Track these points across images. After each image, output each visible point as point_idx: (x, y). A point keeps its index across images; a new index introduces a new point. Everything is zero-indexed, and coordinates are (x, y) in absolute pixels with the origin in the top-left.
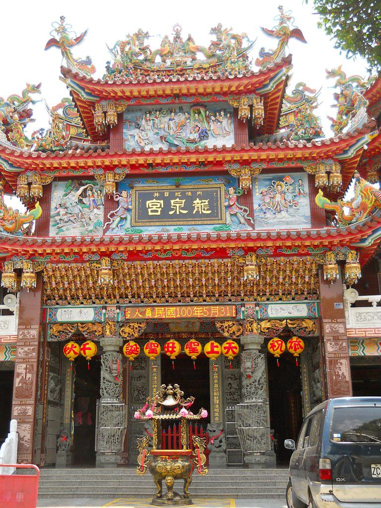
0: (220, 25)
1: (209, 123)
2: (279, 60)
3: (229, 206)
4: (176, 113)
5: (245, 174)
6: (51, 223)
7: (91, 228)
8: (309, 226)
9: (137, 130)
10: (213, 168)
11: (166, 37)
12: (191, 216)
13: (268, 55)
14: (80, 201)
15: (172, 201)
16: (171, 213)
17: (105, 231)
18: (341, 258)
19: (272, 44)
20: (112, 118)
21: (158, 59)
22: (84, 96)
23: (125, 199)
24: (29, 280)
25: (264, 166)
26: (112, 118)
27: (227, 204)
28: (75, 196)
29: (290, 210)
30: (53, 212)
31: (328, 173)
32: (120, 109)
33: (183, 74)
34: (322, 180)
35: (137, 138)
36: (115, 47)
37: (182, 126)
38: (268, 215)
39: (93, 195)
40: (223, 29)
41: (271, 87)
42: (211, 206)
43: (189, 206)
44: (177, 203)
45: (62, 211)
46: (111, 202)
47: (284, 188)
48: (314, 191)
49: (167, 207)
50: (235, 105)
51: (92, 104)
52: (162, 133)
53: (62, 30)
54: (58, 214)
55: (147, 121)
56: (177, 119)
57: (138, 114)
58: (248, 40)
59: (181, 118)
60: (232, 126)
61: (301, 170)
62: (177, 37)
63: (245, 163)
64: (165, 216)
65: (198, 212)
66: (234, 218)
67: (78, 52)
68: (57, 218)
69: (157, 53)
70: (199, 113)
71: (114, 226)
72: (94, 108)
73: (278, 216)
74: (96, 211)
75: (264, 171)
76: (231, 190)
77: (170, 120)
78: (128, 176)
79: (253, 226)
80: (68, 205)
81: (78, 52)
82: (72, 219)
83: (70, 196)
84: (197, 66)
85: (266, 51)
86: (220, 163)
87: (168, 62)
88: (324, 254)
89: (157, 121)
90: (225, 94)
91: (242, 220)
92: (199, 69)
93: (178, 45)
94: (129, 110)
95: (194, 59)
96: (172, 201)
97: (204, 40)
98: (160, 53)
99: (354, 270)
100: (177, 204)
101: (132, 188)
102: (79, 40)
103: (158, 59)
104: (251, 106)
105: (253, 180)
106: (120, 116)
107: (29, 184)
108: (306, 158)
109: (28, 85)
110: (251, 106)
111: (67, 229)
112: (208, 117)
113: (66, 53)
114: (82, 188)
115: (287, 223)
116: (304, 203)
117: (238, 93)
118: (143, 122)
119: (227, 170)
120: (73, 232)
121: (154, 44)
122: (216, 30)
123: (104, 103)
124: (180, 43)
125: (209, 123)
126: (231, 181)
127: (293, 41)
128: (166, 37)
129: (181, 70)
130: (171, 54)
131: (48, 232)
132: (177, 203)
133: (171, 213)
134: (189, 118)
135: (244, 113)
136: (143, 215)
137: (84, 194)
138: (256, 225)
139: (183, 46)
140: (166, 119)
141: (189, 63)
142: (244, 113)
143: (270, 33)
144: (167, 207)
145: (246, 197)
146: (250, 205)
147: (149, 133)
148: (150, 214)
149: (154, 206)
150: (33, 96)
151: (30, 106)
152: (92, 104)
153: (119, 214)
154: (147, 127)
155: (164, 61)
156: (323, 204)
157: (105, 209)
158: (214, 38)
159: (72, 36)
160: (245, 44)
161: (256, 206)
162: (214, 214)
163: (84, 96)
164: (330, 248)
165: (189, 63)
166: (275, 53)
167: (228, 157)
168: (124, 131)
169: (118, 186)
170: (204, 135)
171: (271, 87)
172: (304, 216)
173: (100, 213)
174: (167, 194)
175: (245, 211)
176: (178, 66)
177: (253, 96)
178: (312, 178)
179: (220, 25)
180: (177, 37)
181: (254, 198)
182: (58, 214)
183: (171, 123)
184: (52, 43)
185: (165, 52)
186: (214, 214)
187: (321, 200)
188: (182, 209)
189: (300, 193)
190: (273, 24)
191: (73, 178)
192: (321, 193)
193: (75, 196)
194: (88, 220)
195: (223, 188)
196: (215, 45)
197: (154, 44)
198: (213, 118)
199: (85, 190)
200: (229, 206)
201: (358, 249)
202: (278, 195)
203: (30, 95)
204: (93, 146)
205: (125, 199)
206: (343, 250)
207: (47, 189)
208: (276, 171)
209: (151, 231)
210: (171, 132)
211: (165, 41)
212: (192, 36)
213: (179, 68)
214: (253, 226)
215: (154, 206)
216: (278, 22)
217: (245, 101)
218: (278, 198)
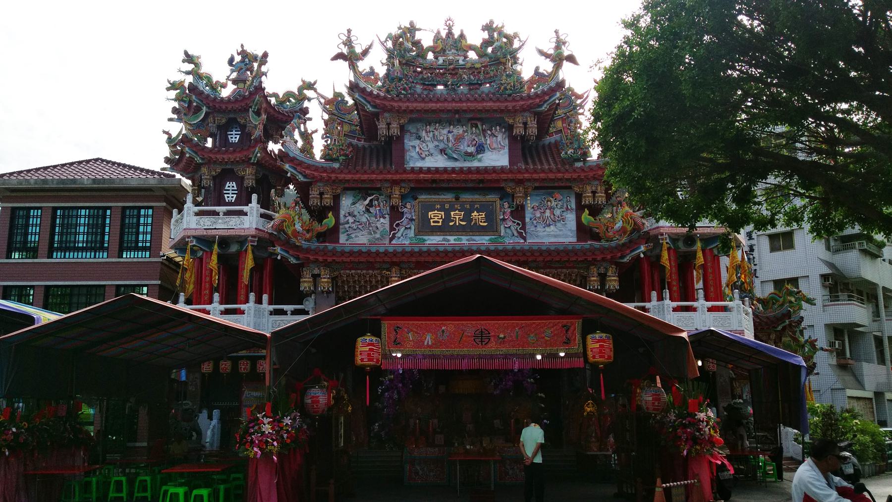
0: (492, 22)
1: (485, 137)
2: (553, 84)
3: (504, 220)
4: (455, 126)
5: (520, 191)
6: (341, 231)
7: (378, 236)
8: (574, 240)
9: (418, 142)
10: (486, 183)
11: (439, 33)
12: (472, 229)
13: (542, 75)
14: (368, 211)
15: (452, 213)
16: (451, 224)
17: (391, 239)
18: (602, 271)
19: (547, 66)
20: (395, 130)
21: (430, 56)
22: (369, 108)
23: (410, 211)
24: (325, 282)
25: (537, 185)
26: (395, 130)
27: (502, 217)
28: (360, 207)
29: (558, 224)
30: (342, 220)
31: (594, 193)
32: (402, 121)
33: (456, 74)
34: (588, 200)
35: (417, 149)
36: (386, 40)
37: (459, 139)
38: (538, 229)
39: (379, 205)
40: (494, 26)
41: (545, 107)
42: (488, 219)
43: (467, 217)
44: (456, 214)
45: (351, 220)
46: (396, 215)
47: (554, 204)
48: (580, 208)
49: (447, 218)
50: (511, 121)
51: (376, 116)
52: (442, 146)
53: (348, 43)
54: (348, 223)
55: (427, 132)
56: (455, 131)
57: (419, 125)
58: (520, 40)
59: (459, 130)
60: (507, 141)
61: (570, 188)
62: (450, 33)
63: (520, 182)
64: (445, 229)
65: (475, 223)
66: (508, 230)
67: (363, 66)
68: (347, 226)
69: (430, 49)
70: (476, 127)
71: (399, 235)
72: (378, 120)
73: (547, 229)
74: (382, 220)
75: (536, 188)
76: (506, 205)
77: (449, 132)
78: (412, 189)
79: (525, 239)
80: (356, 213)
81: (363, 66)
82: (360, 227)
83: (357, 205)
84: (469, 65)
85: (541, 71)
86: (498, 181)
87: (441, 60)
88: (588, 268)
89: (436, 133)
90: (502, 111)
91: (516, 234)
92: (470, 68)
93: (450, 41)
94: (412, 121)
95: (466, 57)
96: (452, 213)
97: (476, 37)
98: (432, 49)
99: (613, 283)
100: (457, 216)
101: (416, 199)
102: (365, 53)
103: (430, 56)
104: (525, 124)
105: (526, 195)
106: (402, 128)
107: (321, 194)
108: (575, 179)
109: (304, 82)
110: (525, 124)
111: (356, 236)
112: (484, 131)
113: (353, 67)
114: (369, 199)
115: (555, 236)
116: (571, 217)
117: (514, 112)
118: (424, 134)
119: (503, 188)
120: (362, 239)
121: (426, 40)
122: (488, 28)
123: (387, 115)
124: (450, 43)
125: (485, 137)
126: (504, 195)
127: (566, 65)
128: (439, 33)
129: (454, 69)
130: (443, 51)
131: (338, 239)
132: (456, 214)
133: (451, 224)
134: (466, 131)
135: (519, 131)
136: (425, 227)
137: (370, 204)
138: (528, 237)
139: (455, 43)
140: (445, 131)
141: (461, 62)
142: (519, 131)
143: (547, 56)
144: (447, 218)
145: (518, 213)
146: (523, 219)
147: (429, 144)
148: (432, 224)
149: (436, 217)
150: (309, 93)
151: (306, 104)
152: (376, 116)
153: (404, 224)
154: (427, 139)
155: (436, 58)
156: (588, 222)
157: (390, 218)
158: (486, 35)
159: (358, 50)
160: (516, 44)
161: (527, 220)
162: (491, 228)
163: (369, 108)
164: (594, 262)
165: (461, 62)
166: (550, 74)
167: (504, 176)
168: (405, 141)
169: (403, 197)
170: (480, 149)
171: (545, 107)
172: (570, 230)
173: (386, 221)
174: (447, 206)
175: (518, 224)
176: (450, 64)
177: (527, 114)
178: (579, 197)
179: (492, 22)
180: (450, 33)
181: (526, 212)
182: (348, 223)
183: (450, 135)
184: (340, 56)
185: (438, 49)
186: (491, 228)
187: (586, 217)
188: (461, 220)
189: (567, 209)
190: (550, 49)
191: (360, 189)
192: (587, 211)
193: (360, 207)
194: (375, 229)
195: (498, 202)
196: (486, 43)
197: (426, 40)
198: (489, 132)
199: (371, 201)
200: (504, 220)
201: (617, 264)
202: (548, 212)
203: (305, 92)
204: (367, 145)
205: (410, 211)
206: (605, 265)
207: (337, 199)
208: (548, 187)
209: (433, 240)
210: (450, 145)
211: (437, 38)
212: (465, 33)
213: (451, 67)
214: (525, 239)
215: (436, 217)
216: (554, 45)
217: (519, 119)
218: (548, 213)
